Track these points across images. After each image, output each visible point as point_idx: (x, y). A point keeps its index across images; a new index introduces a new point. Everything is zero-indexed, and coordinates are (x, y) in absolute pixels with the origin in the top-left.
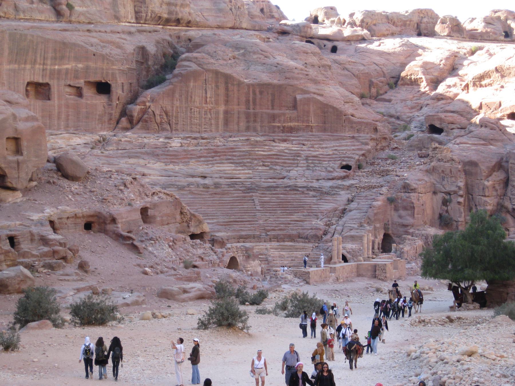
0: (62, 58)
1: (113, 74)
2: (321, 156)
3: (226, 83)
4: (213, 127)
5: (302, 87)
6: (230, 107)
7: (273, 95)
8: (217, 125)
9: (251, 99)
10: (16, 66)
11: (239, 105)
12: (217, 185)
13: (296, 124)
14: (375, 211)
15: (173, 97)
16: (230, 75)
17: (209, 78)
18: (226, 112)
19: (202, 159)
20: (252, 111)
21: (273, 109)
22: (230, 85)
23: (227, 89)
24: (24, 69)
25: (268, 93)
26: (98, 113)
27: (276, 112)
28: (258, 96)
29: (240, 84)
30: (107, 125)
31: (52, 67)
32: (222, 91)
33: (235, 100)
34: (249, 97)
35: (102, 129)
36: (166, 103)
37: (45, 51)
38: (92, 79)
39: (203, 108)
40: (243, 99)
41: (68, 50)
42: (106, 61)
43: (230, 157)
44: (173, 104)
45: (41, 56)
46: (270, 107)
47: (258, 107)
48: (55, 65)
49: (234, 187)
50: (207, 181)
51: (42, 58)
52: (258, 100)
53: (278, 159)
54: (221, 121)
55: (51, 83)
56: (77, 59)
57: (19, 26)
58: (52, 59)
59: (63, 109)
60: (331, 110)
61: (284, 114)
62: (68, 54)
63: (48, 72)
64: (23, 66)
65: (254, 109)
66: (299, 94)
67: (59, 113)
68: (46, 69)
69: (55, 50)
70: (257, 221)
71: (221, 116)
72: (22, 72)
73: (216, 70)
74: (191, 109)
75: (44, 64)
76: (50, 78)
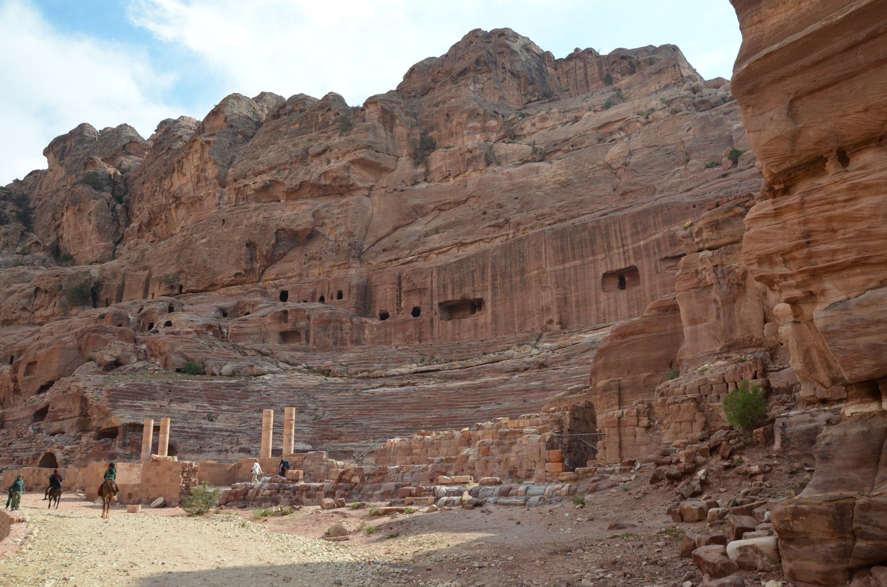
0: (645, 230)
10: (577, 262)
24: (594, 262)
31: (636, 245)
41: (651, 216)
45: (617, 238)
48: (639, 240)
51: (620, 240)
55: (637, 264)
58: (632, 235)
62: (652, 222)
63: (631, 253)
64: (591, 258)
68: (628, 250)
69: (634, 225)
72: (592, 265)
75: (623, 246)
76: (636, 259)
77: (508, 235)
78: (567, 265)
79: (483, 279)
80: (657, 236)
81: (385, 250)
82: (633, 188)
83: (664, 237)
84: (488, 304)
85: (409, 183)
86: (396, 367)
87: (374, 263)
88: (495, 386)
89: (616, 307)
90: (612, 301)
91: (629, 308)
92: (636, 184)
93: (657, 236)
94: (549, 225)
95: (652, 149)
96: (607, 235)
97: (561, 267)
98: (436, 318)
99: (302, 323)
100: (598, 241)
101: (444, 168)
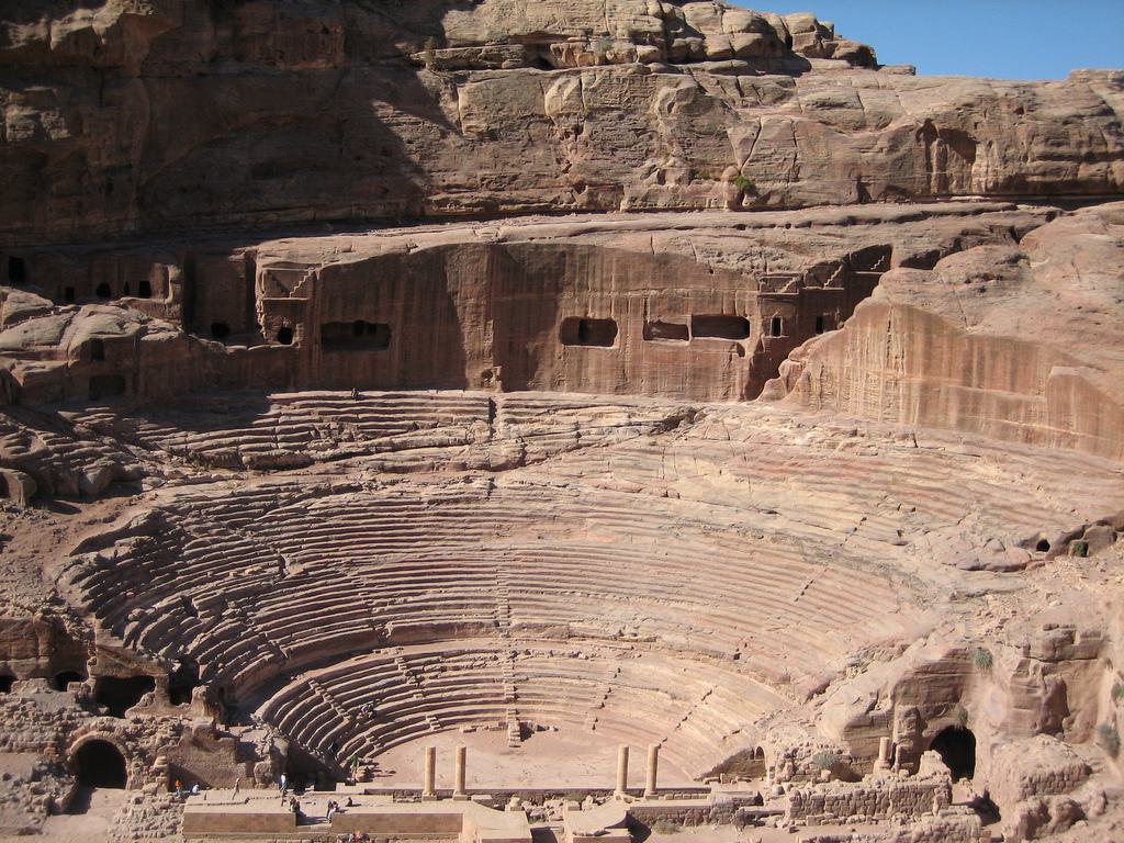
0: (639, 277)
1: (751, 303)
2: (1022, 510)
3: (928, 331)
4: (902, 414)
5: (1066, 351)
6: (935, 378)
7: (1014, 361)
8: (909, 409)
9: (975, 365)
10: (533, 296)
11: (950, 376)
12: (779, 536)
13: (1047, 427)
14: (909, 676)
15: (842, 350)
16: (936, 316)
17: (895, 320)
18: (925, 388)
19: (811, 478)
20: (973, 389)
21: (1013, 389)
22: (934, 336)
23: (929, 343)
25: (1005, 358)
26: (721, 370)
27: (1018, 396)
28: (988, 362)
29: (955, 335)
30: (738, 391)
31: (622, 295)
32: (919, 347)
33: (943, 365)
34: (971, 361)
35: (726, 397)
36: (833, 363)
37: (602, 269)
38: (711, 311)
39: (885, 375)
40: (960, 364)
42: (737, 283)
43: (856, 482)
44: (842, 362)
46: (1008, 386)
47: (986, 382)
49: (801, 545)
50: (774, 525)
51: (598, 280)
52: (987, 369)
53: (937, 500)
54: (916, 404)
57: (547, 231)
58: (619, 280)
59: (646, 363)
60: (1109, 407)
61: (1028, 404)
65: (979, 386)
66: (1058, 365)
67: (634, 368)
69: (623, 268)
70: (760, 626)
71: (916, 394)
73: (909, 306)
74: (868, 376)
75: (602, 290)
77: (398, 205)
78: (518, 297)
79: (392, 297)
80: (653, 292)
81: (184, 190)
82: (594, 179)
83: (661, 297)
84: (396, 334)
85: (207, 59)
86: (304, 447)
87: (164, 213)
88: (477, 500)
89: (580, 367)
90: (575, 359)
91: (598, 373)
92: (597, 173)
93: (653, 292)
94: (467, 205)
95: (615, 114)
96: (582, 267)
97: (510, 299)
98: (316, 348)
99: (128, 363)
100: (568, 274)
101: (270, 43)
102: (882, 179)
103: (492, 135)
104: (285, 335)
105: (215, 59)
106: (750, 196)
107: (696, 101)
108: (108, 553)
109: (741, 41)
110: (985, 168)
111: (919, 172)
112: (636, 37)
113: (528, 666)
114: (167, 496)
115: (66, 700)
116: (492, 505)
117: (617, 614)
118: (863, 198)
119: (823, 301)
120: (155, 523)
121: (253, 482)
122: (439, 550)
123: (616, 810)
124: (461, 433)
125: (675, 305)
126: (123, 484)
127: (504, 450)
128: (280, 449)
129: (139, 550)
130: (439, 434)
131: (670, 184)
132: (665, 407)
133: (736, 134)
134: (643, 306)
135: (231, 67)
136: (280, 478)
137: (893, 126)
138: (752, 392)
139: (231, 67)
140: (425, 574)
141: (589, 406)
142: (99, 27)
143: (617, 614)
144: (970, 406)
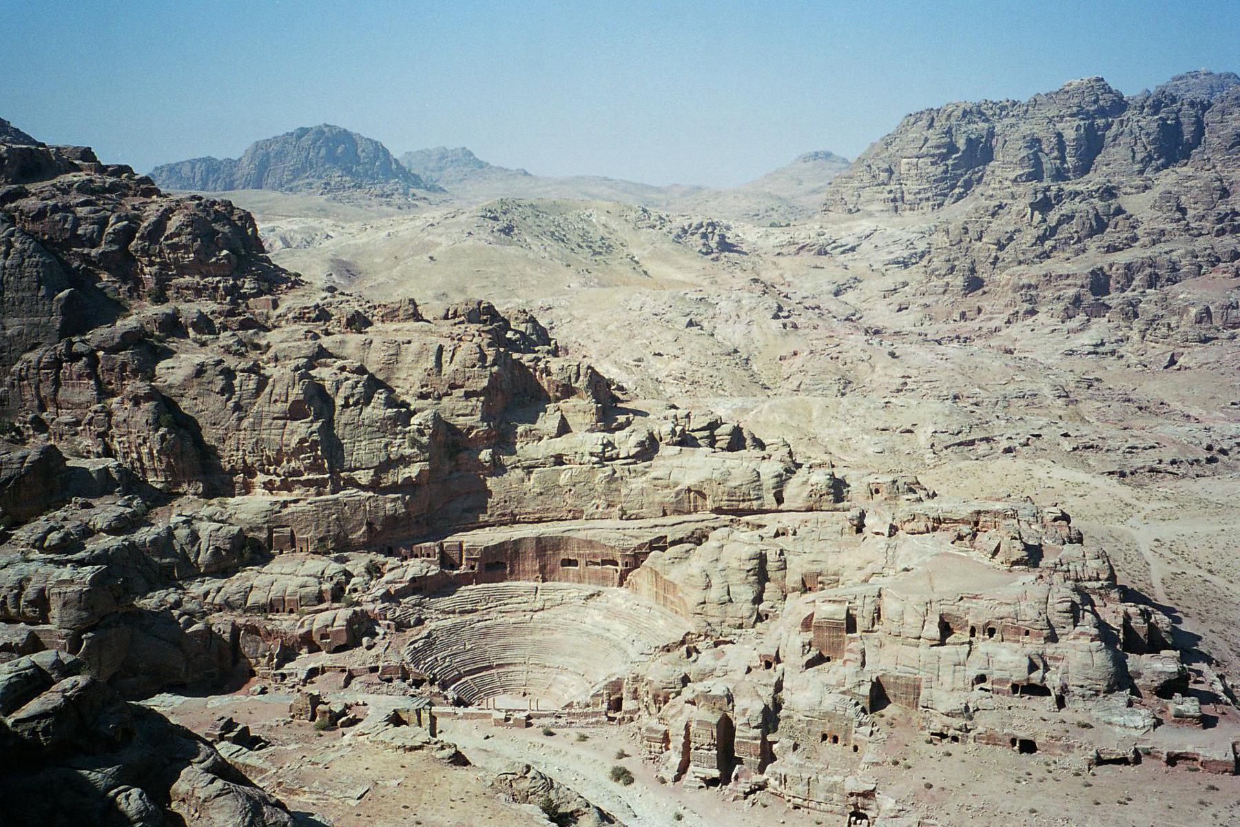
50: (608, 634)
56: (593, 547)
102: (672, 508)
103: (541, 494)
104: (472, 568)
105: (450, 473)
106: (624, 515)
107: (612, 479)
108: (416, 645)
109: (633, 451)
110: (709, 503)
111: (686, 505)
112: (592, 454)
113: (531, 675)
114: (433, 625)
115: (405, 685)
116: (531, 625)
117: (558, 660)
118: (665, 514)
119: (636, 559)
120: (429, 635)
121: (459, 619)
122: (512, 640)
123: (526, 714)
124: (525, 599)
125: (595, 556)
126: (420, 622)
127: (538, 605)
128: (469, 607)
129: (425, 643)
130: (519, 599)
131: (600, 509)
132: (590, 589)
133: (624, 491)
134: (584, 556)
135: (456, 475)
136: (468, 617)
137: (679, 488)
138: (621, 584)
139: (456, 475)
140: (506, 647)
141: (567, 588)
142: (413, 475)
143: (558, 660)
144: (665, 598)
